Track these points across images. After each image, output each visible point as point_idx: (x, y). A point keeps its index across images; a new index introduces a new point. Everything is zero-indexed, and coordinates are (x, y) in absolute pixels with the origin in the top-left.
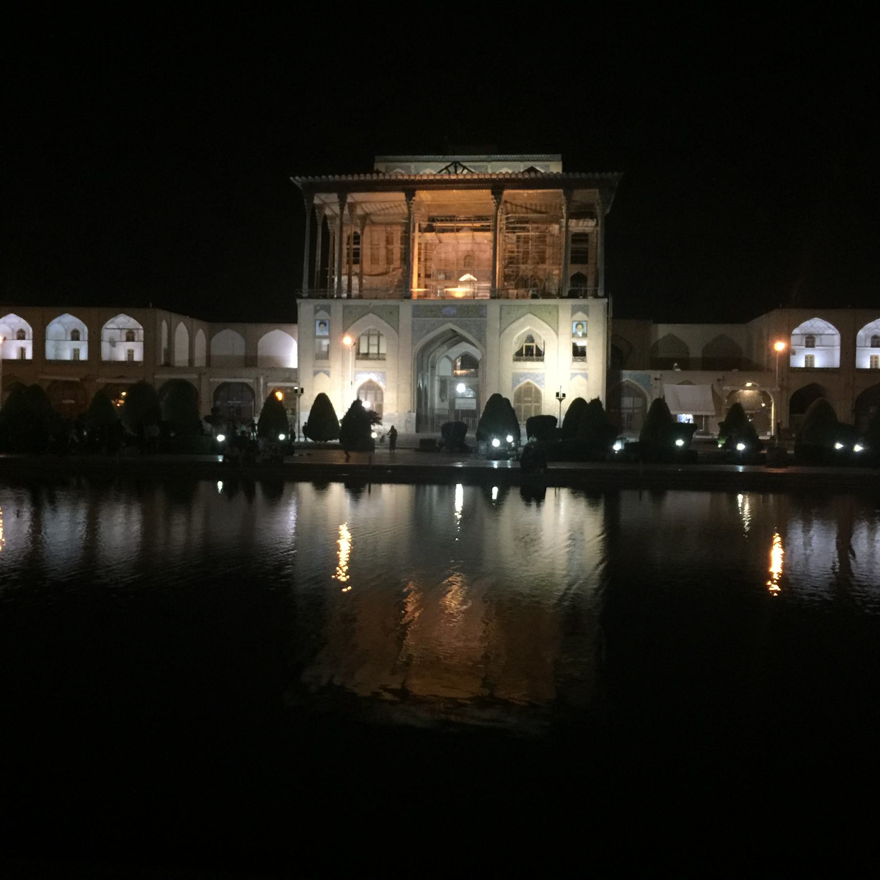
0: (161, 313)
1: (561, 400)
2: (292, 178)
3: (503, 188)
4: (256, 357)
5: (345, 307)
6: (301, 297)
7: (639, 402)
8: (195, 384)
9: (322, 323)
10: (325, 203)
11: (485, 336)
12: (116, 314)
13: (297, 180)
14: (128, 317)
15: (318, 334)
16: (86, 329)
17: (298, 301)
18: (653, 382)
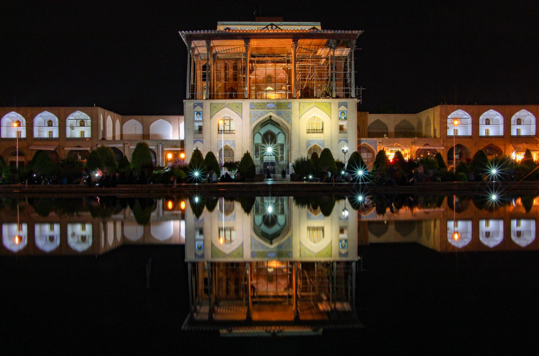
0: (100, 110)
1: (345, 153)
2: (180, 32)
3: (299, 38)
4: (149, 134)
5: (211, 104)
6: (186, 99)
7: (370, 155)
8: (121, 150)
9: (199, 113)
10: (196, 47)
11: (291, 119)
12: (74, 111)
13: (183, 34)
14: (81, 112)
15: (195, 119)
16: (57, 120)
17: (184, 101)
18: (378, 143)
